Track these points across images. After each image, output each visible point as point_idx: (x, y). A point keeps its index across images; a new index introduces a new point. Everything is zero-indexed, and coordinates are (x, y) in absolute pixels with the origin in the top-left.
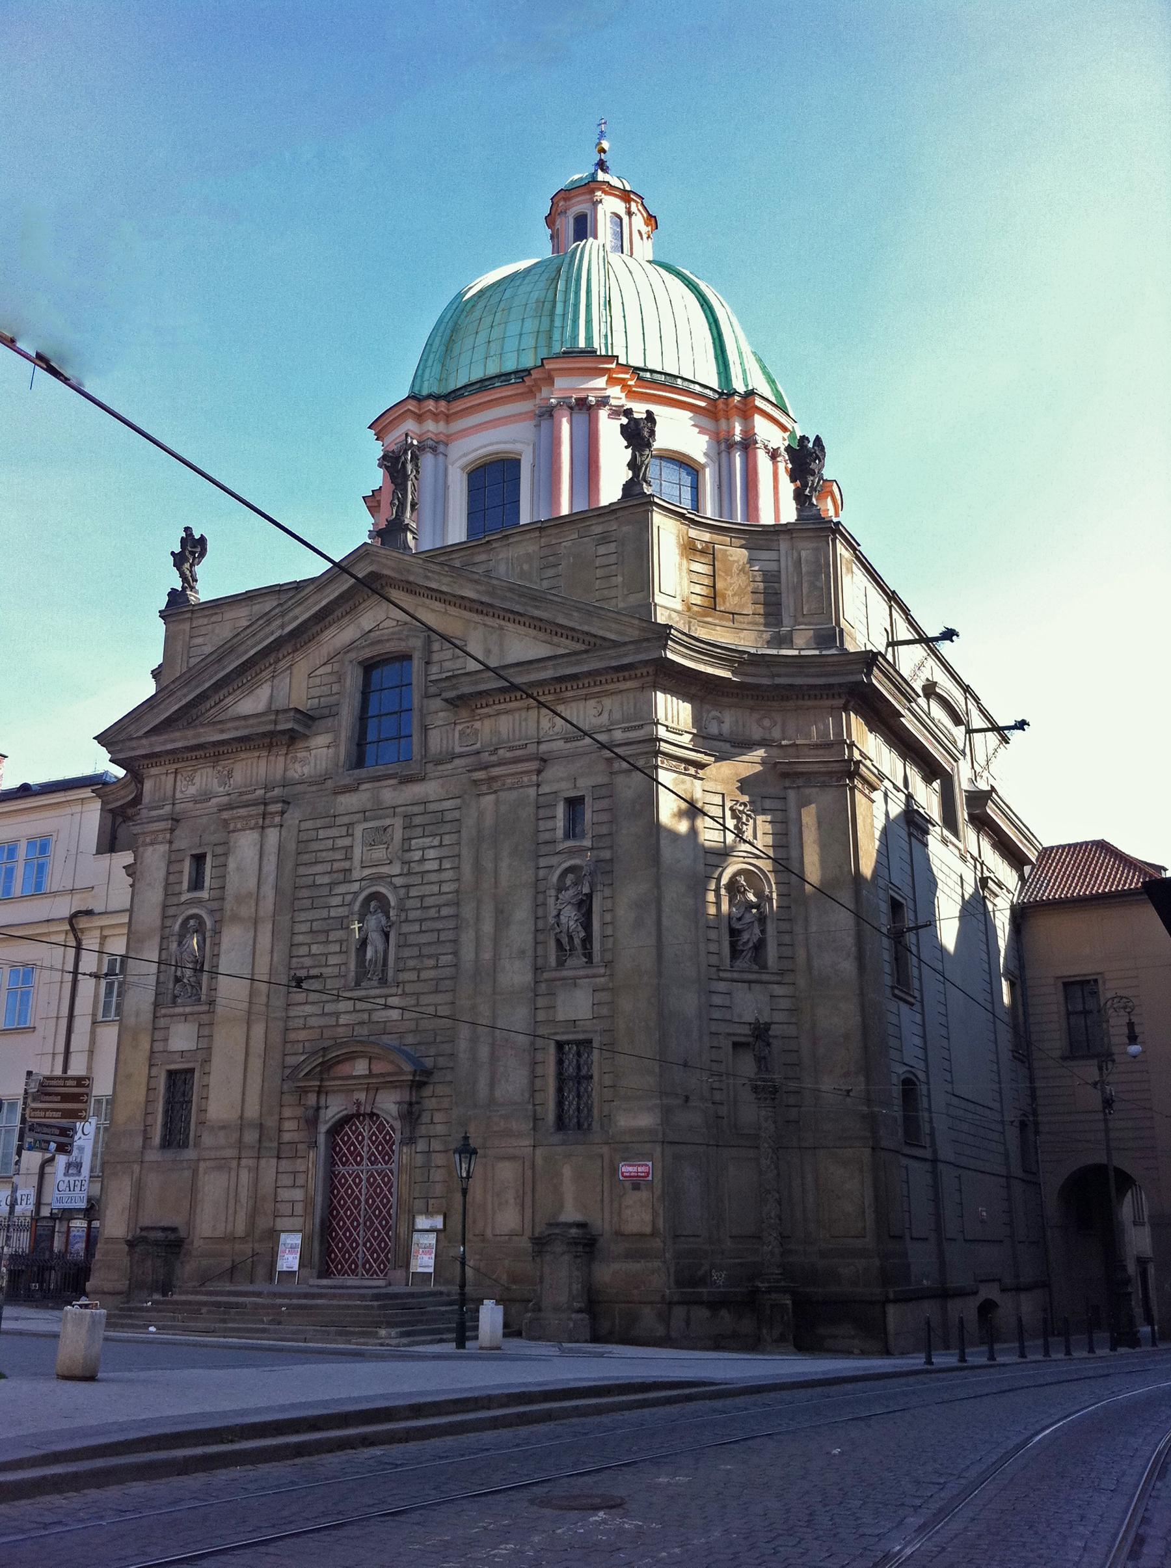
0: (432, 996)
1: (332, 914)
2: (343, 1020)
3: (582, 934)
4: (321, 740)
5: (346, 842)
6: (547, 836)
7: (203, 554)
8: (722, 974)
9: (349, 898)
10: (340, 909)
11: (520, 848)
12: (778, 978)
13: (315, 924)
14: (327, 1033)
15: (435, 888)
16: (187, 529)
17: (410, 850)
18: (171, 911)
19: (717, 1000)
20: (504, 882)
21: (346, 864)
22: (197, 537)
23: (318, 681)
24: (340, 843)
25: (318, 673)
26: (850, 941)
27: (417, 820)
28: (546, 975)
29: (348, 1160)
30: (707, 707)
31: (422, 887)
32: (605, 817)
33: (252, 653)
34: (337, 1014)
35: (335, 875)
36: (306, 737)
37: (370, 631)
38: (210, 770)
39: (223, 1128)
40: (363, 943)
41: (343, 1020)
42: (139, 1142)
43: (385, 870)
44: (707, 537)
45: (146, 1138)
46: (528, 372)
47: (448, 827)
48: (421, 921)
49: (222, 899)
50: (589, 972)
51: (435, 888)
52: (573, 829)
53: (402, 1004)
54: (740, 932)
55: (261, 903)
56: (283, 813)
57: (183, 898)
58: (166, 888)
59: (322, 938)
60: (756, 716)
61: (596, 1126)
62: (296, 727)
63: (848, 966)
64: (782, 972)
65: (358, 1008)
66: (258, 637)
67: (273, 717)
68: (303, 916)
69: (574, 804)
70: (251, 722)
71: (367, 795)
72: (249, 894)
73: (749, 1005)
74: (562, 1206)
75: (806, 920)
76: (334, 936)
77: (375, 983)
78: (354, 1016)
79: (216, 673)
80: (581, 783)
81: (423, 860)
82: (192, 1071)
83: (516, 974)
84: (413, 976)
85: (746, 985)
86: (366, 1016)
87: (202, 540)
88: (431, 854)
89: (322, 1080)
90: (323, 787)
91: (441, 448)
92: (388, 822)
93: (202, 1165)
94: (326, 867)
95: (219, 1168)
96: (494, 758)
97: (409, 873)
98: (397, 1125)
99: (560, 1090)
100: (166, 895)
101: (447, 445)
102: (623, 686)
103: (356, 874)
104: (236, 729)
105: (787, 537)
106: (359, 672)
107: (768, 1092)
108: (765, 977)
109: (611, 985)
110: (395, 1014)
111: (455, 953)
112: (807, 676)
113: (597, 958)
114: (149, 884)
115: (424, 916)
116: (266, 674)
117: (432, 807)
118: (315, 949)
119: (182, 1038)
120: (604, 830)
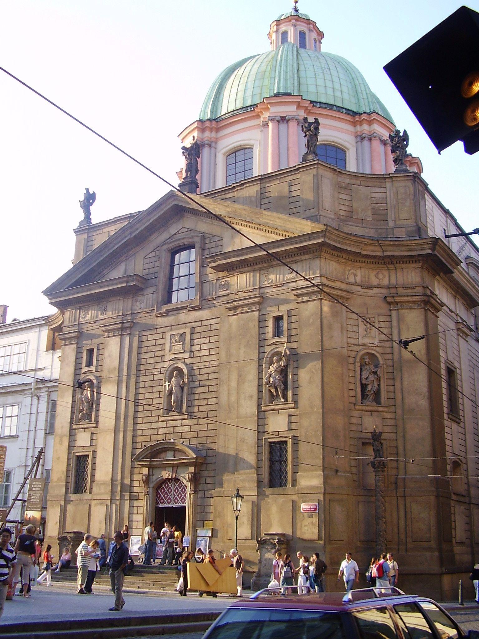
2: (161, 431)
4: (151, 290)
7: (94, 201)
8: (357, 407)
11: (250, 343)
12: (386, 409)
16: (87, 190)
19: (354, 420)
22: (91, 192)
23: (148, 261)
24: (159, 342)
25: (148, 256)
26: (424, 389)
27: (197, 330)
29: (164, 501)
30: (348, 268)
33: (116, 247)
36: (142, 289)
37: (174, 235)
38: (96, 306)
39: (103, 484)
40: (171, 393)
41: (161, 431)
42: (64, 490)
44: (348, 181)
45: (67, 489)
46: (256, 105)
47: (213, 333)
50: (286, 406)
52: (278, 332)
54: (366, 385)
56: (130, 328)
57: (83, 371)
58: (75, 367)
59: (150, 390)
60: (375, 273)
61: (289, 485)
62: (137, 284)
63: (424, 403)
64: (388, 406)
66: (119, 240)
67: (126, 279)
69: (278, 319)
70: (115, 282)
71: (173, 317)
72: (115, 368)
73: (371, 424)
74: (271, 526)
75: (402, 379)
76: (156, 389)
79: (98, 259)
82: (88, 456)
83: (249, 408)
85: (369, 413)
87: (94, 194)
88: (205, 347)
89: (150, 461)
90: (151, 314)
91: (213, 145)
93: (93, 503)
94: (152, 354)
95: (101, 504)
96: (237, 297)
98: (188, 484)
99: (271, 467)
100: (75, 369)
101: (216, 143)
102: (303, 257)
103: (168, 357)
104: (108, 286)
105: (390, 180)
106: (169, 256)
107: (379, 466)
108: (380, 409)
109: (297, 413)
110: (187, 429)
112: (401, 251)
114: (67, 364)
116: (123, 258)
118: (147, 396)
119: (83, 439)
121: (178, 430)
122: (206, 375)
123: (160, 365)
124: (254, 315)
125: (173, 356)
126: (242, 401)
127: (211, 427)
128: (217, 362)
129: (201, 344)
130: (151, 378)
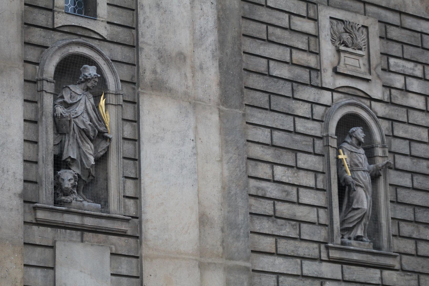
1: (301, 126)
5: (308, 26)
9: (319, 111)
10: (310, 124)
13: (276, 134)
17: (387, 70)
18: (37, 36)
21: (312, 61)
27: (394, 33)
31: (411, 128)
35: (298, 71)
48: (413, 173)
49: (134, 46)
55: (199, 75)
57: (61, 20)
65: (347, 277)
68: (258, 117)
72: (182, 57)
81: (405, 90)
84: (409, 246)
88: (415, 85)
92: (361, 20)
97: (390, 103)
103: (329, 79)
115: (414, 169)
117: (409, 22)
118: (280, 173)
125: (341, 82)
129: (405, 76)
130: (287, 123)
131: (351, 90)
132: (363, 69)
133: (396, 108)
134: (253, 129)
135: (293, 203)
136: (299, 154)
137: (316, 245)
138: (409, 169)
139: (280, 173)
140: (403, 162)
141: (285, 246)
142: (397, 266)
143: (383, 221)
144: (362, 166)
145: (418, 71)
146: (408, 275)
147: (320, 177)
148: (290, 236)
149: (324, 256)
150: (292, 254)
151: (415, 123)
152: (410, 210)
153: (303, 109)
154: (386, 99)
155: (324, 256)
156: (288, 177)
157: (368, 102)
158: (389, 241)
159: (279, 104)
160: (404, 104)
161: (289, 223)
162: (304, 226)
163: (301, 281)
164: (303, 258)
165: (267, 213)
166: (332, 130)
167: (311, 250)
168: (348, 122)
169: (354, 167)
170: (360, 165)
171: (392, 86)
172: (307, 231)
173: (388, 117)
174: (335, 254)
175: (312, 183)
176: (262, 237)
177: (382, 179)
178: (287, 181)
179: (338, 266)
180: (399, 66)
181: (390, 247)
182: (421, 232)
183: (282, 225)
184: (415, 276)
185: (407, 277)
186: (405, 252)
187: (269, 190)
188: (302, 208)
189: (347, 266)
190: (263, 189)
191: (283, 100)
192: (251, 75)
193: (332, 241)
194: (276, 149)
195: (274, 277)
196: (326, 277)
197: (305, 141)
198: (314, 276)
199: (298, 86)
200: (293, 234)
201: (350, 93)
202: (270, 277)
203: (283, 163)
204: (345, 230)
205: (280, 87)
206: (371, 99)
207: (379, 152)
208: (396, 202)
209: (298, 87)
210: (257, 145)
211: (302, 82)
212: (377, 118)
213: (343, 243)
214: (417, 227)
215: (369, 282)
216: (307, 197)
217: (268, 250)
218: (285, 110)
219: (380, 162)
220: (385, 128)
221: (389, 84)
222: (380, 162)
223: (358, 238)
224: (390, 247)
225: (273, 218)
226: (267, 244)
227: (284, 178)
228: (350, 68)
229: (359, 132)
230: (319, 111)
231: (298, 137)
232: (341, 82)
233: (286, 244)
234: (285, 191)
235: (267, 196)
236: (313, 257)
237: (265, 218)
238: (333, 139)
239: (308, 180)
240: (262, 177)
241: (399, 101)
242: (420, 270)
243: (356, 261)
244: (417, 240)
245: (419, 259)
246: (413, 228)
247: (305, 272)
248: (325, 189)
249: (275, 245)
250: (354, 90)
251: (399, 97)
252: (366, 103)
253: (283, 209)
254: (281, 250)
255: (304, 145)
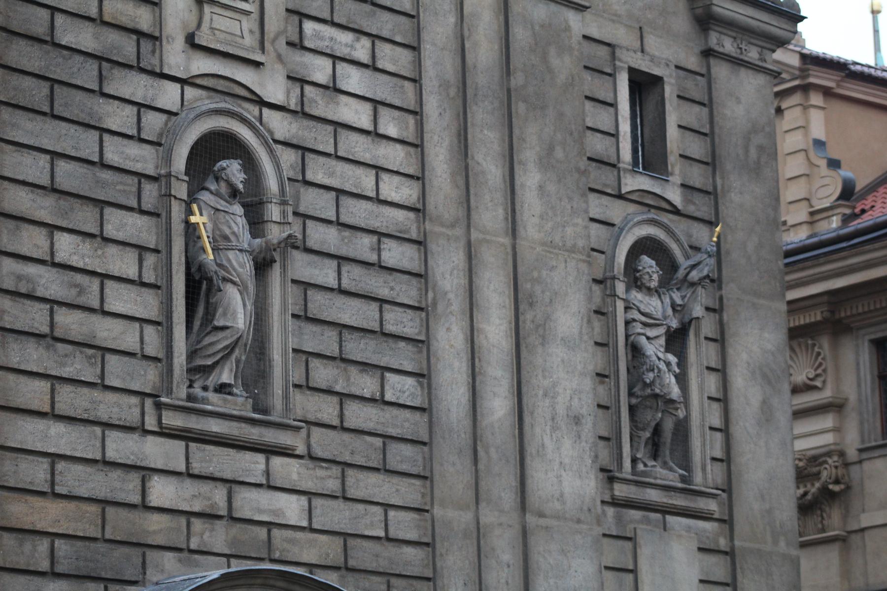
0: (373, 478)
3: (681, 414)
6: (598, 145)
10: (134, 150)
11: (559, 153)
13: (62, 166)
14: (120, 523)
15: (366, 181)
17: (298, 45)
20: (532, 228)
28: (621, 491)
31: (340, 166)
32: (697, 148)
34: (145, 472)
35: (113, 37)
41: (162, 491)
43: (244, 75)
47: (385, 24)
51: (366, 181)
53: (308, 485)
59: (86, 218)
65: (197, 467)
77: (239, 404)
78: (190, 487)
80: (651, 42)
81: (333, 89)
83: (567, 472)
84: (327, 409)
86: (219, 495)
88: (353, 80)
97: (302, 113)
103: (176, 58)
109: (723, 543)
110: (292, 509)
111: (423, 376)
113: (698, 478)
115: (343, 251)
118: (67, 247)
120: (697, 176)
121: (254, 503)
122: (367, 241)
123: (136, 86)
124: (568, 29)
125: (202, 65)
126: (540, 432)
127: (404, 525)
128: (405, 192)
131: (222, 82)
132: (249, 40)
133: (312, 123)
134: (15, 154)
135: (91, 310)
136: (108, 210)
137: (134, 400)
138: (332, 251)
139: (67, 247)
140: (322, 236)
141: (70, 400)
142: (301, 449)
143: (276, 356)
144: (238, 240)
145: (362, 50)
146: (322, 467)
147: (150, 260)
148: (83, 379)
149: (151, 423)
150: (85, 416)
151: (351, 157)
152: (331, 334)
153: (119, 118)
154: (293, 105)
155: (151, 423)
156: (83, 257)
157: (255, 110)
158: (286, 397)
159: (72, 103)
160: (330, 118)
161: (81, 352)
162: (112, 361)
163: (101, 473)
164: (107, 425)
165: (37, 329)
166: (180, 163)
167: (126, 409)
168: (214, 148)
169: (221, 242)
170: (232, 238)
171: (308, 79)
172: (117, 371)
173: (295, 141)
174: (173, 420)
175: (132, 272)
176: (23, 379)
177: (277, 267)
178: (81, 265)
179: (179, 446)
180: (322, 39)
181: (287, 409)
182: (352, 380)
183: (66, 356)
184: (336, 470)
185: (321, 473)
186: (317, 421)
187: (43, 281)
188: (109, 322)
189: (198, 445)
190: (29, 279)
191: (79, 96)
192: (14, 42)
193: (169, 392)
194: (60, 198)
195: (45, 463)
196: (152, 466)
197: (121, 183)
198: (129, 462)
199: (112, 69)
200: (89, 375)
201: (220, 88)
202: (38, 461)
203: (75, 228)
204: (196, 371)
205: (75, 70)
206: (262, 103)
207: (274, 212)
208: (304, 317)
209: (113, 71)
210: (22, 187)
211: (120, 60)
212: (273, 143)
213: (190, 398)
214: (345, 370)
215: (241, 479)
216: (121, 299)
217: (35, 406)
218: (83, 117)
219: (275, 234)
220: (288, 164)
221: (301, 73)
222: (275, 234)
223: (222, 388)
224: (287, 409)
225: (48, 339)
226: (34, 393)
227: (75, 258)
228: (222, 36)
229: (234, 170)
230: (153, 122)
231: (106, 175)
232: (202, 65)
233: (72, 395)
234: (76, 286)
235: (39, 294)
236: (128, 424)
237: (32, 339)
238: (180, 182)
239: (125, 264)
240: (28, 254)
241: (319, 110)
242: (347, 458)
243: (216, 435)
244: (343, 397)
245: (346, 437)
246: (336, 371)
247: (111, 455)
248: (159, 284)
249: (49, 397)
250: (227, 83)
251: (320, 102)
252: (251, 111)
253: (70, 322)
254: (62, 408)
255: (120, 191)
